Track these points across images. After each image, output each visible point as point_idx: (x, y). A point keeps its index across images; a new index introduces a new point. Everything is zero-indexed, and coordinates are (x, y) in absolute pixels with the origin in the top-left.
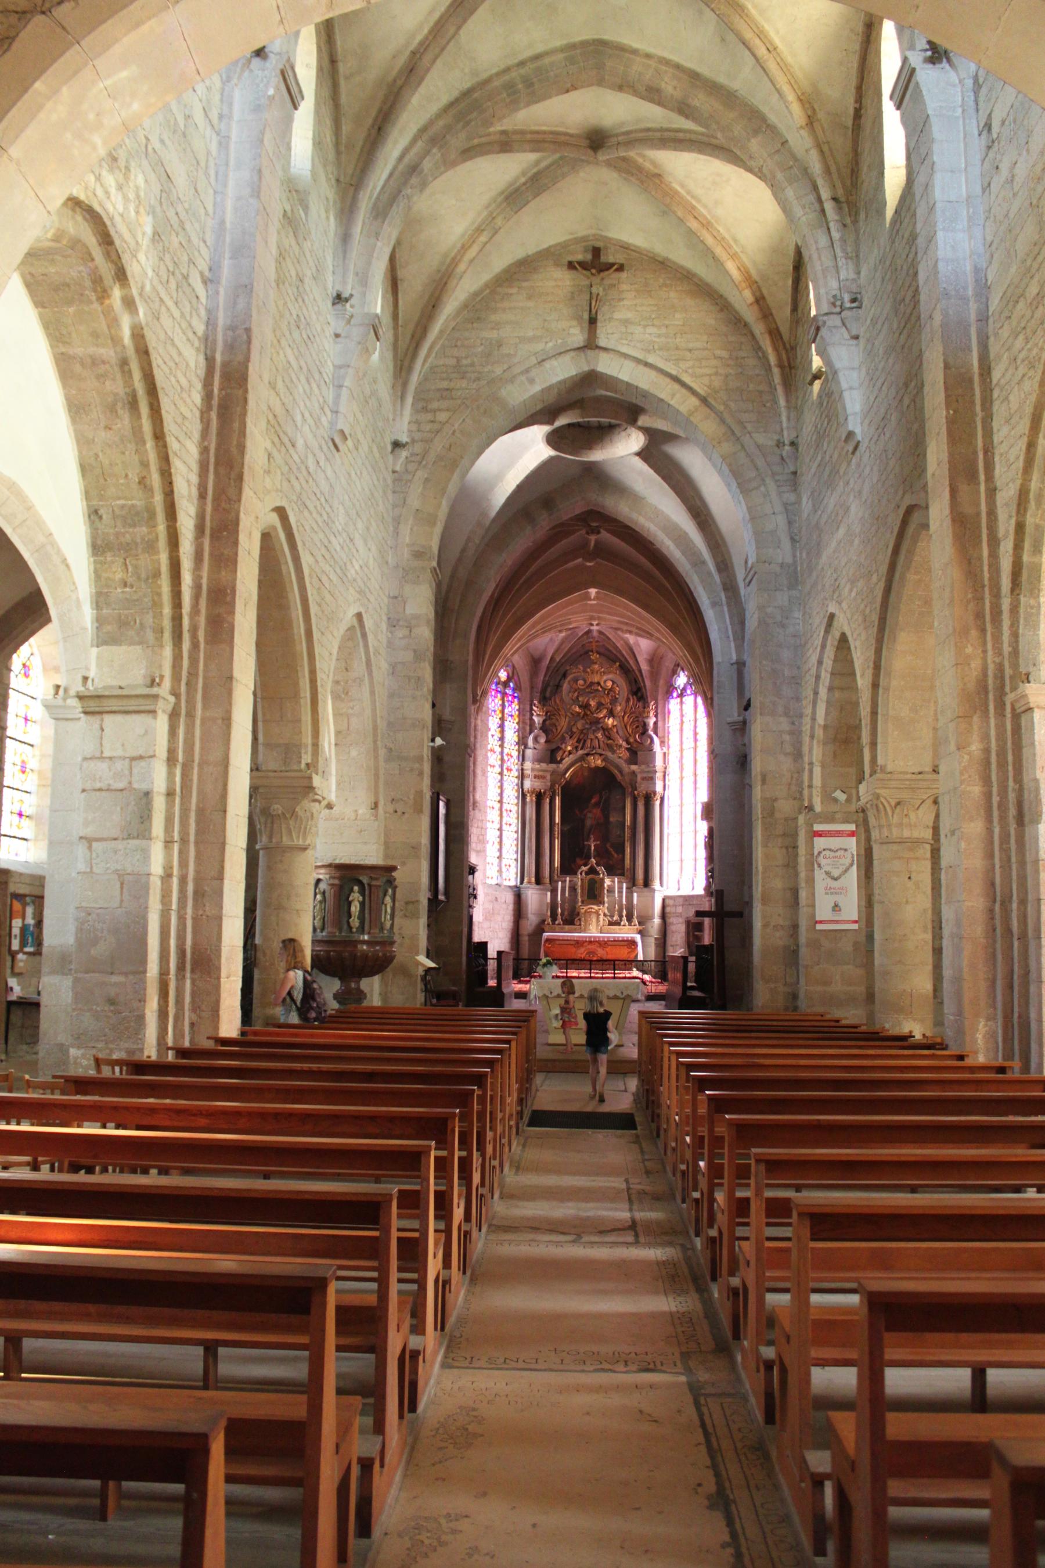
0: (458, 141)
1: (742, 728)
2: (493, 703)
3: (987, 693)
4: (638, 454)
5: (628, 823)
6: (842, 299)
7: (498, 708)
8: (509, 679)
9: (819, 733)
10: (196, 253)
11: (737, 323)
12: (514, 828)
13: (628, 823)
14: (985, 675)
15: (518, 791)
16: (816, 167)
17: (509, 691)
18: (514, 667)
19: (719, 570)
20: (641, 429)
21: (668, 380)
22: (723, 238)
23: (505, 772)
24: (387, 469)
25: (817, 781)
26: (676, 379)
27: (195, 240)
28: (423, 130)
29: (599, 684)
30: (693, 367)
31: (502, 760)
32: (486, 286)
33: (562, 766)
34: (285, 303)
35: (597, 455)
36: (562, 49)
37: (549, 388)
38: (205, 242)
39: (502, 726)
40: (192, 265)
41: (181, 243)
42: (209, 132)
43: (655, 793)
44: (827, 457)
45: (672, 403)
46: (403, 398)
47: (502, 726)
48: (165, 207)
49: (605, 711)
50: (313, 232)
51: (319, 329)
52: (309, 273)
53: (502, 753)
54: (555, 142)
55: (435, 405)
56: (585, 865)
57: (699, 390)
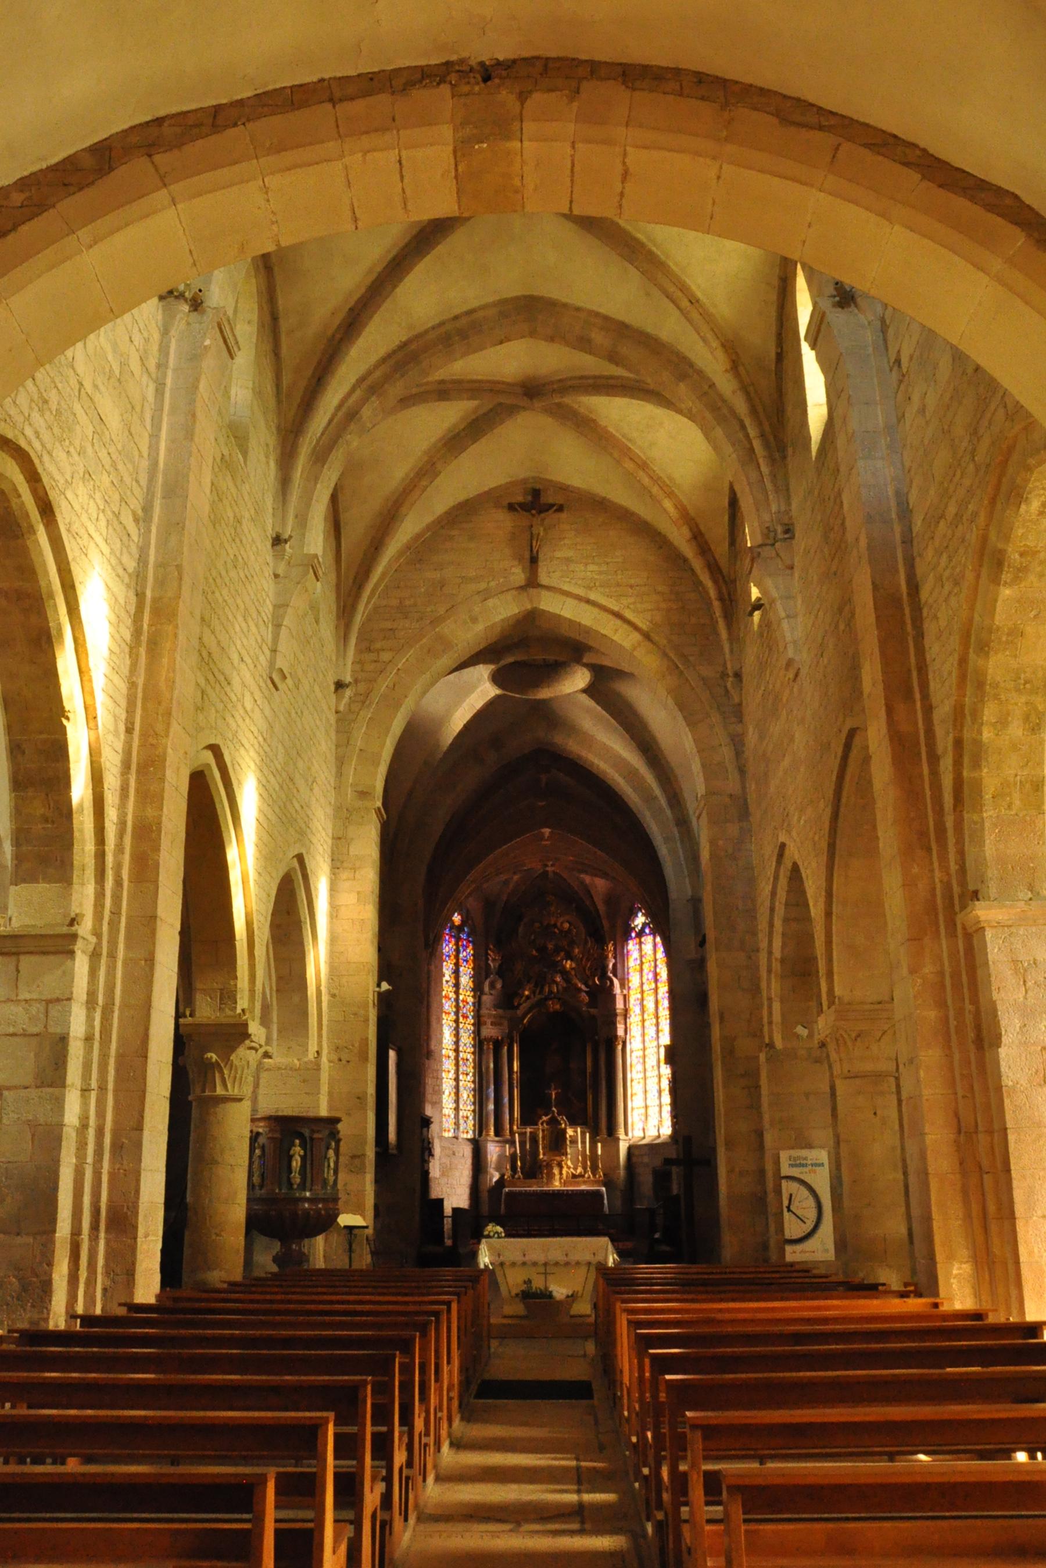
0: (396, 390)
1: (700, 965)
2: (448, 947)
3: (936, 915)
4: (584, 691)
5: (589, 1070)
6: (775, 531)
7: (453, 953)
8: (464, 922)
9: (776, 966)
10: (129, 493)
11: (674, 559)
12: (470, 1078)
13: (589, 1070)
14: (934, 895)
15: (474, 1039)
16: (741, 406)
17: (463, 936)
18: (468, 911)
19: (671, 806)
20: (587, 666)
21: (610, 617)
22: (660, 478)
23: (461, 1019)
24: (330, 709)
25: (777, 1017)
26: (618, 615)
27: (127, 479)
28: (362, 380)
29: (555, 926)
30: (634, 603)
31: (457, 1007)
32: (428, 528)
33: (520, 1012)
34: (221, 544)
35: (544, 694)
36: (495, 304)
37: (493, 626)
38: (137, 481)
39: (456, 973)
40: (123, 504)
41: (112, 482)
42: (145, 379)
43: (616, 1037)
44: (771, 686)
45: (615, 638)
46: (346, 638)
47: (456, 973)
48: (96, 447)
49: (562, 954)
50: (252, 475)
51: (258, 568)
52: (247, 515)
53: (457, 1000)
54: (491, 390)
55: (378, 645)
56: (546, 1115)
57: (640, 624)
